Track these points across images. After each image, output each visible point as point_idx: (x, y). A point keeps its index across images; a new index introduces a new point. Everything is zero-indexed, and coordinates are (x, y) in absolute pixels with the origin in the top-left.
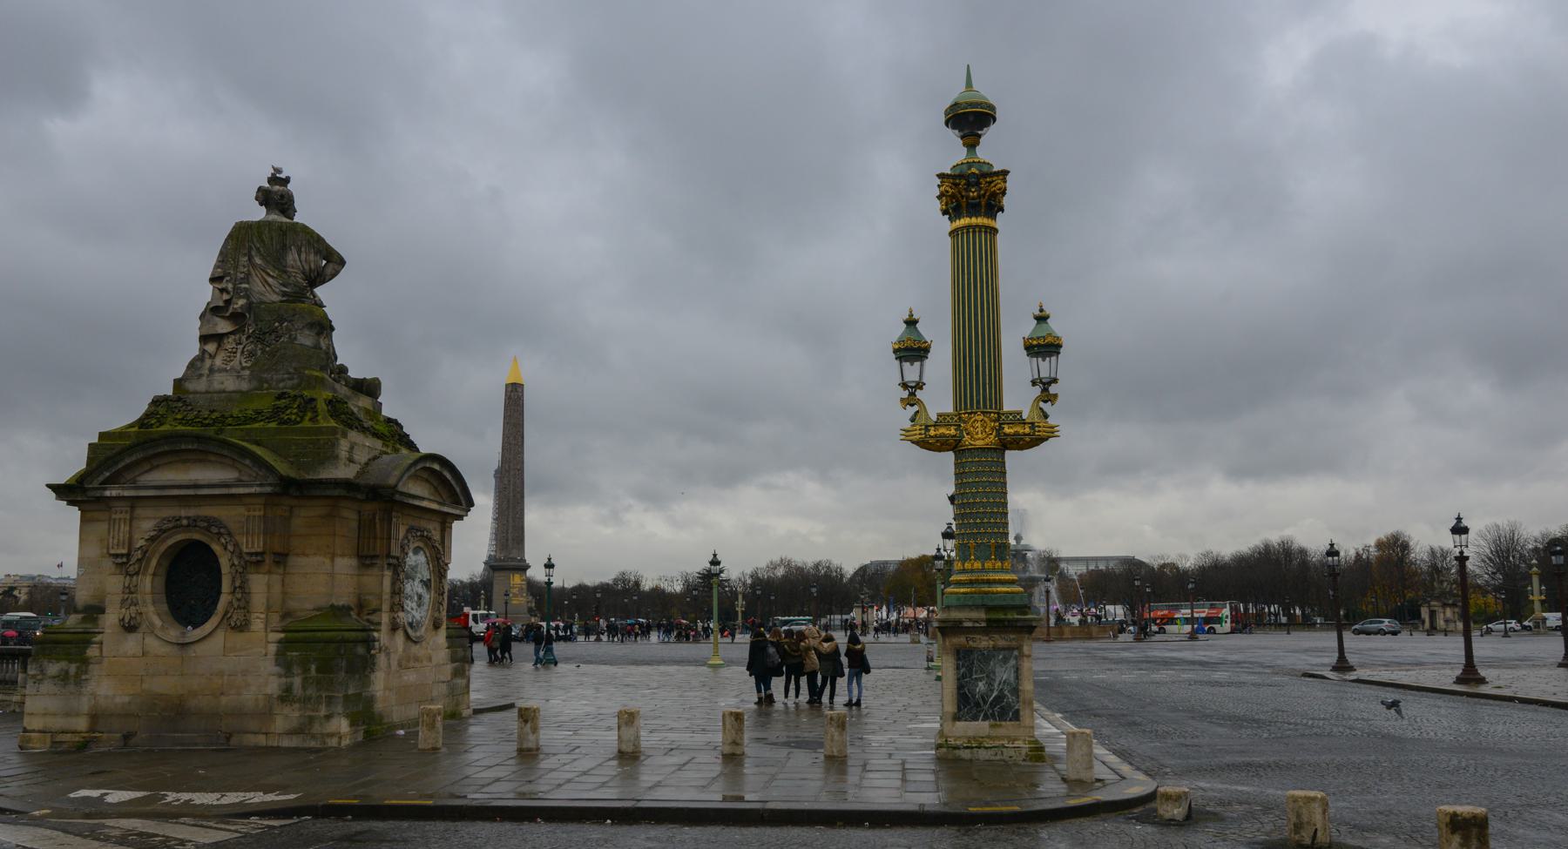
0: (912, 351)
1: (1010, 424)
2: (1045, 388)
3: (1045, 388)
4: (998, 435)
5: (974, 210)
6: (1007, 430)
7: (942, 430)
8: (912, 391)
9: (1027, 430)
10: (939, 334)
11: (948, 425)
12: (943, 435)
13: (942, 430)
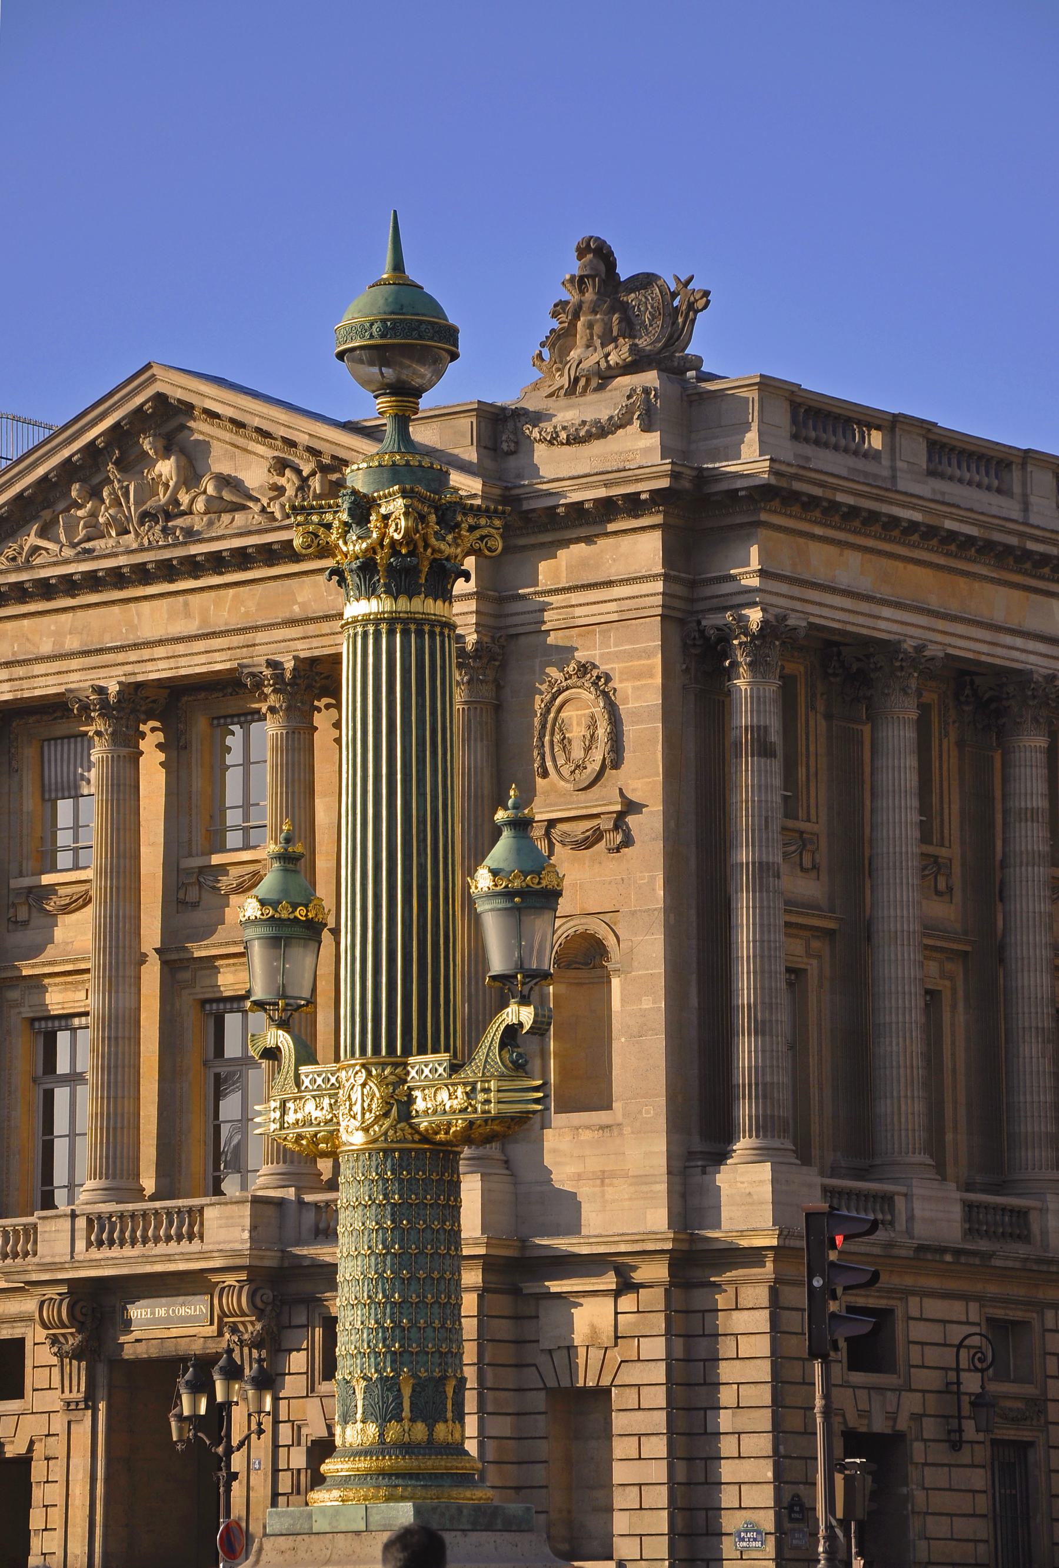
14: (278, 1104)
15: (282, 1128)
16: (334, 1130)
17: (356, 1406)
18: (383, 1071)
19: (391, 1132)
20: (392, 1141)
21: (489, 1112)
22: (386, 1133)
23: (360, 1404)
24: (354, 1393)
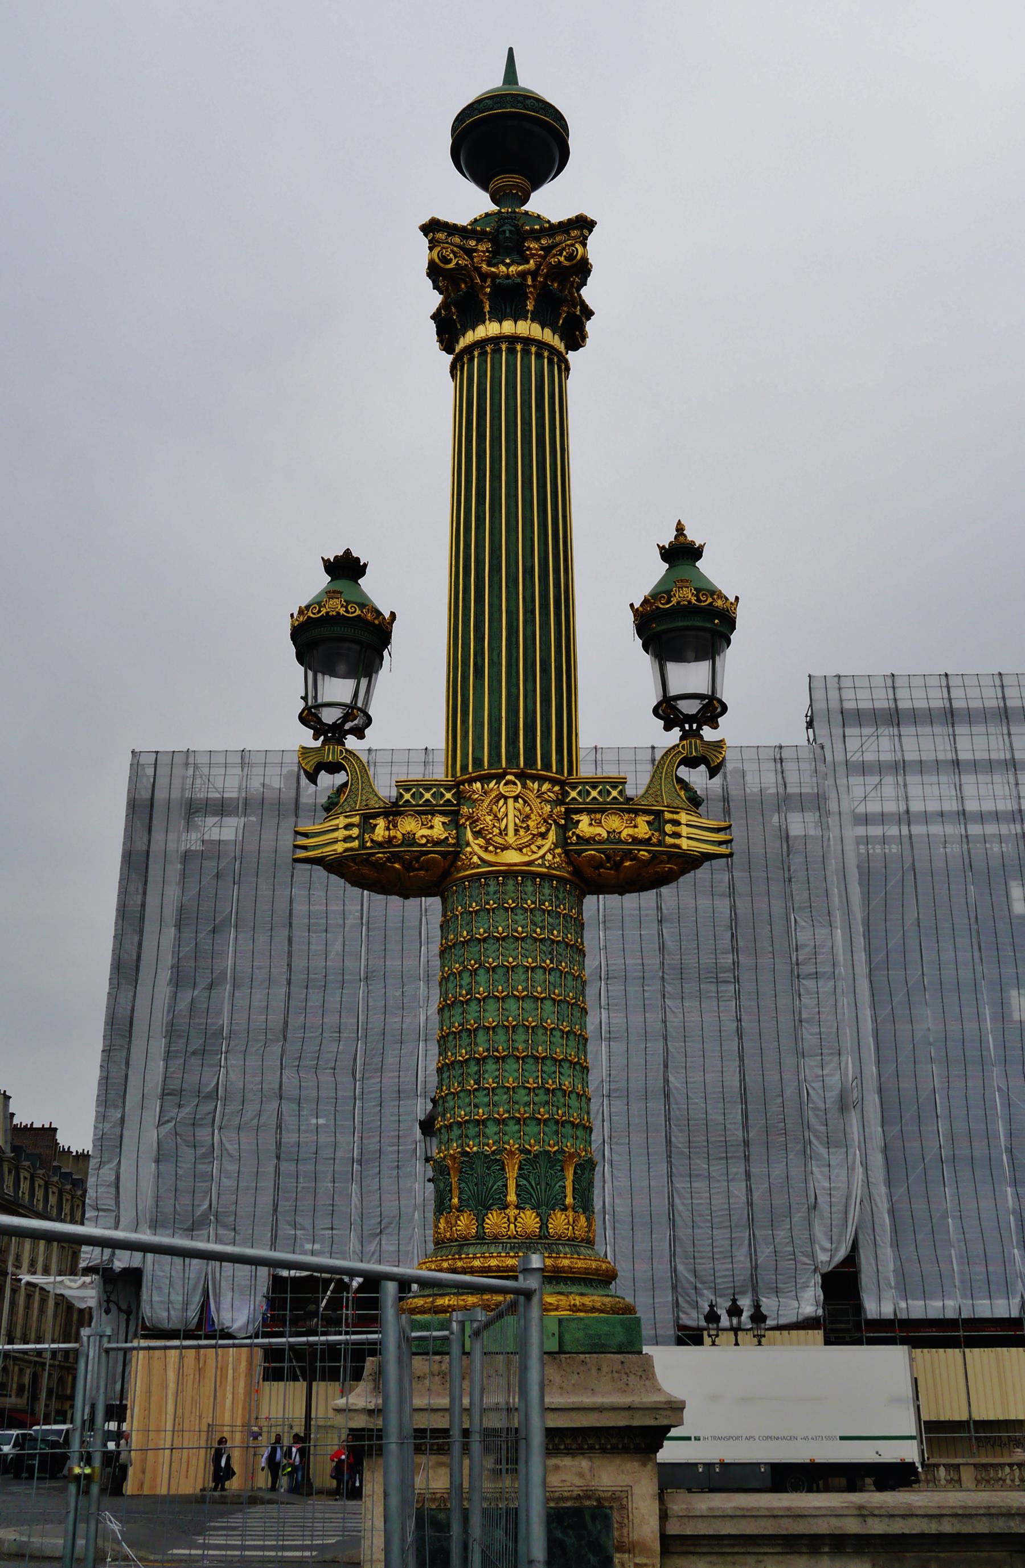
0: (342, 636)
1: (597, 810)
2: (691, 718)
3: (691, 718)
4: (563, 842)
5: (508, 301)
6: (585, 826)
7: (408, 825)
8: (334, 731)
9: (642, 829)
10: (415, 590)
11: (426, 811)
12: (409, 839)
13: (408, 825)
14: (356, 820)
15: (363, 846)
17: (506, 1186)
18: (540, 786)
19: (549, 857)
21: (678, 847)
22: (543, 857)
23: (512, 1185)
24: (503, 1169)
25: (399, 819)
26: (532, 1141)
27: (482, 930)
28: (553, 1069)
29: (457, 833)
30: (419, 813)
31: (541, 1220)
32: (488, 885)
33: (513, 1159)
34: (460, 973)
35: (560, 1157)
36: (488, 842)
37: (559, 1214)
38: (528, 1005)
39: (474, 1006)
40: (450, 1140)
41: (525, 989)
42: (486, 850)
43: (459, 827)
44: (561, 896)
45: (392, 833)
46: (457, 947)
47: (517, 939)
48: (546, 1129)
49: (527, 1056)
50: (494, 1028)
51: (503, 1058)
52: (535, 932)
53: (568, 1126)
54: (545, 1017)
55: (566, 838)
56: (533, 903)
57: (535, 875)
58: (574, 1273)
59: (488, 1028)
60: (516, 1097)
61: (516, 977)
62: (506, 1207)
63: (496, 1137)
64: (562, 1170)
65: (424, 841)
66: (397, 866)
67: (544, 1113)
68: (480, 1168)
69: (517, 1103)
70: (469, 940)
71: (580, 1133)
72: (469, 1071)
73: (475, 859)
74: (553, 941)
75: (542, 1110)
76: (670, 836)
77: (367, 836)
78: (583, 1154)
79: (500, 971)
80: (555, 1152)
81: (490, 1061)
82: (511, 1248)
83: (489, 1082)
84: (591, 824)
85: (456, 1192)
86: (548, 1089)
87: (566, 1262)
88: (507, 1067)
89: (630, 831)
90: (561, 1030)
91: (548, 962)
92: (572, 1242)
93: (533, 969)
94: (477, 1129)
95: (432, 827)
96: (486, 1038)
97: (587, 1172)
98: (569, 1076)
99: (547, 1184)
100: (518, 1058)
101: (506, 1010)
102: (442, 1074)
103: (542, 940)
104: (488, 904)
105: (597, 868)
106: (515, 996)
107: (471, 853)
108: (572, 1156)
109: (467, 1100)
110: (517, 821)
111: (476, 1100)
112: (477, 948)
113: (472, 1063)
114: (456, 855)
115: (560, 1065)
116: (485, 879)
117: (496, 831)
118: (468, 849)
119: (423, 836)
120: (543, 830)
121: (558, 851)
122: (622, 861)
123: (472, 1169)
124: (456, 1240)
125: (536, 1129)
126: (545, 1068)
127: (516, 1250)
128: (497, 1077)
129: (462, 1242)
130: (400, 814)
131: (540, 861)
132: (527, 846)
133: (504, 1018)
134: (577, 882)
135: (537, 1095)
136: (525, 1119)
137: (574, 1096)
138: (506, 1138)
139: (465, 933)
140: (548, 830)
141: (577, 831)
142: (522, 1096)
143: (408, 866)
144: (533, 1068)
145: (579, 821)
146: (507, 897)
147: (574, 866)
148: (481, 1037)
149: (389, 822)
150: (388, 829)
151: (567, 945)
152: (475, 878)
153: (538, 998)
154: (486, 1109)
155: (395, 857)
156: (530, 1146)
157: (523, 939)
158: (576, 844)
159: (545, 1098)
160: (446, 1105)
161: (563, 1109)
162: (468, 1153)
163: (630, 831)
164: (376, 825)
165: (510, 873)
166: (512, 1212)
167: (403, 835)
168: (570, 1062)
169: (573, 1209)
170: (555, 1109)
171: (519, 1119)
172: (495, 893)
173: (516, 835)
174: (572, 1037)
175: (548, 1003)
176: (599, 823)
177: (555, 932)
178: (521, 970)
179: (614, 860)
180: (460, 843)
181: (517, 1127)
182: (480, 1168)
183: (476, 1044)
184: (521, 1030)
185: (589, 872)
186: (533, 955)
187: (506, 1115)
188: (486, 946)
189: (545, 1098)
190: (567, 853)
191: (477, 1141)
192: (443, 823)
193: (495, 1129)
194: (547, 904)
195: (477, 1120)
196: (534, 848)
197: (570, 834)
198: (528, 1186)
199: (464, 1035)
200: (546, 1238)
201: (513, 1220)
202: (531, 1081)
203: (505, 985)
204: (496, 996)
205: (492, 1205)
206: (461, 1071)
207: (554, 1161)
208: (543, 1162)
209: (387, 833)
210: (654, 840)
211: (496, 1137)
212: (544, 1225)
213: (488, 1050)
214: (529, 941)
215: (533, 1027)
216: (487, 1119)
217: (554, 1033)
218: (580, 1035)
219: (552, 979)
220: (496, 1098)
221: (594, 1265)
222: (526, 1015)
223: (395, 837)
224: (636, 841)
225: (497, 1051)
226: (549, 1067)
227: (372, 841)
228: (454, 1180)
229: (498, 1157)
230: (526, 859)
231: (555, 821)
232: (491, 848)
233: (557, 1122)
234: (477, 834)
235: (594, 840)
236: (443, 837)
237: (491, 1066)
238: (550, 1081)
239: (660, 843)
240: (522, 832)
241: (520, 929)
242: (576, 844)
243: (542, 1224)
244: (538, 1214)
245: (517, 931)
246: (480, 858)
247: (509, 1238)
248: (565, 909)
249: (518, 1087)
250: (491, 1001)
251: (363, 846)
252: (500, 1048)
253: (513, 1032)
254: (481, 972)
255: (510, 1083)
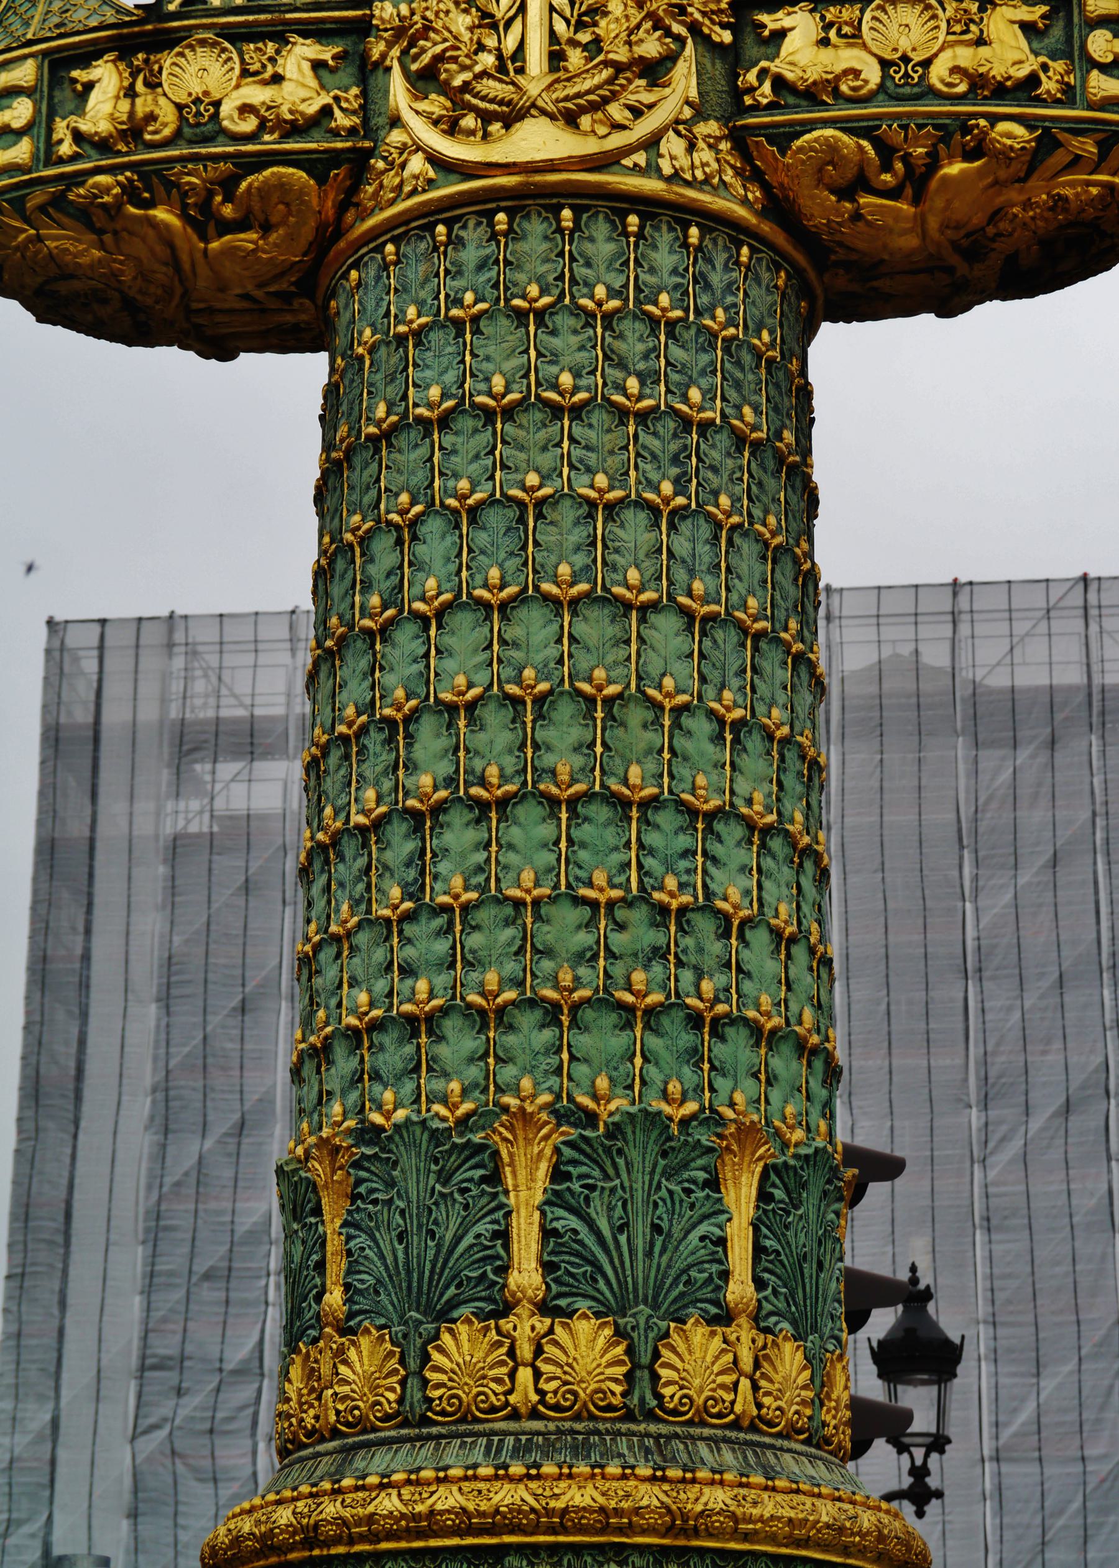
4: (726, 102)
12: (200, 120)
13: (199, 73)
15: (48, 154)
16: (334, 158)
17: (503, 1235)
19: (673, 145)
20: (676, 177)
22: (652, 143)
24: (494, 1178)
25: (167, 60)
26: (602, 1083)
27: (435, 392)
28: (683, 841)
29: (364, 94)
30: (237, 36)
31: (630, 1351)
32: (460, 243)
33: (528, 1142)
34: (365, 541)
35: (705, 1138)
36: (458, 97)
37: (698, 1333)
38: (595, 627)
39: (406, 639)
40: (324, 1098)
41: (583, 573)
42: (452, 129)
43: (368, 72)
44: (717, 279)
45: (143, 106)
46: (357, 461)
47: (556, 411)
48: (654, 1042)
49: (588, 796)
50: (471, 706)
51: (503, 803)
52: (623, 390)
53: (738, 1037)
54: (654, 666)
55: (737, 94)
56: (612, 293)
57: (623, 203)
58: (746, 1537)
59: (452, 709)
60: (546, 934)
61: (549, 535)
62: (505, 1309)
63: (474, 1072)
64: (713, 1184)
65: (249, 125)
66: (161, 214)
67: (645, 985)
68: (414, 1177)
69: (547, 952)
70: (394, 428)
71: (784, 1064)
72: (388, 856)
73: (417, 164)
74: (686, 423)
75: (639, 978)
76: (1104, 68)
77: (61, 129)
78: (798, 1135)
79: (496, 519)
80: (685, 1122)
81: (457, 817)
82: (518, 1452)
83: (452, 885)
84: (824, 42)
85: (336, 1268)
86: (663, 910)
87: (718, 1498)
88: (515, 834)
89: (965, 56)
90: (711, 713)
91: (667, 488)
92: (752, 1433)
93: (612, 510)
94: (409, 1049)
95: (277, 79)
96: (444, 742)
97: (810, 1200)
98: (745, 869)
99: (657, 1229)
100: (554, 802)
101: (516, 645)
102: (310, 883)
103: (642, 417)
104: (458, 302)
105: (847, 192)
106: (547, 598)
107: (402, 149)
108: (747, 1133)
109: (380, 955)
110: (560, 26)
111: (410, 952)
112: (423, 451)
113: (398, 829)
114: (358, 163)
115: (709, 830)
116: (449, 223)
117: (487, 60)
118: (396, 137)
119: (246, 109)
120: (651, 47)
121: (711, 128)
122: (934, 162)
123: (391, 1184)
124: (335, 1434)
125: (618, 1042)
126: (652, 838)
127: (536, 1456)
128: (480, 869)
129: (354, 1435)
130: (167, 41)
131: (640, 158)
132: (594, 107)
133: (508, 672)
134: (780, 239)
135: (621, 927)
136: (575, 1007)
137: (760, 938)
138: (508, 1073)
139: (381, 411)
140: (669, 59)
141: (775, 67)
142: (565, 928)
143: (205, 221)
144: (610, 836)
145: (780, 35)
146: (521, 277)
147: (766, 187)
148: (430, 739)
149: (134, 75)
150: (130, 93)
151: (740, 440)
152: (420, 222)
153: (628, 606)
154: (442, 980)
155: (153, 182)
156: (595, 1097)
157: (577, 412)
158: (772, 106)
159: (654, 937)
160: (318, 982)
161: (721, 980)
162: (381, 1129)
163: (965, 56)
164: (89, 86)
165: (536, 194)
166: (525, 1326)
167: (179, 107)
168: (750, 825)
169: (756, 1319)
170: (687, 976)
171: (556, 1006)
172: (481, 266)
173: (553, 68)
174: (754, 743)
175: (667, 624)
176: (855, 37)
177: (695, 395)
178: (567, 513)
179: (906, 159)
180: (374, 119)
181: (548, 1035)
182: (414, 1177)
183: (412, 767)
184: (565, 710)
185: (821, 206)
186: (613, 462)
187: (510, 995)
188: (448, 440)
189: (654, 937)
190: (739, 139)
191: (409, 1086)
192: (318, 66)
193: (470, 1043)
194: (664, 299)
195: (411, 1020)
196: (616, 111)
197: (752, 77)
198: (584, 1234)
199: (374, 740)
200: (650, 1416)
201: (525, 1351)
202: (600, 878)
203: (512, 564)
204: (480, 602)
205: (453, 1304)
206: (361, 862)
207: (688, 1154)
208: (640, 1154)
209: (125, 106)
210: (1049, 85)
211: (474, 1072)
212: (641, 1368)
213: (450, 781)
214: (598, 417)
215: (609, 701)
216: (445, 1011)
217: (686, 721)
218: (786, 741)
219: (681, 546)
220: (475, 940)
221: (826, 1512)
222: (584, 662)
223: (151, 117)
224: (981, 85)
225: (483, 782)
226: (667, 834)
227: (78, 136)
228: (332, 1226)
229: (477, 1138)
230: (590, 146)
231: (694, 28)
232: (469, 121)
233: (695, 1021)
234: (425, 80)
235: (836, 93)
236: (312, 109)
237: (459, 835)
238: (671, 883)
239: (1069, 95)
240: (575, 58)
241: (566, 379)
242: (772, 106)
243: (636, 1366)
244: (620, 1333)
245: (555, 387)
246: (435, 159)
247: (515, 1415)
248: (731, 322)
249: (553, 900)
250: (463, 620)
251: (48, 154)
252: (493, 772)
253: (539, 716)
254: (433, 526)
255: (525, 883)
